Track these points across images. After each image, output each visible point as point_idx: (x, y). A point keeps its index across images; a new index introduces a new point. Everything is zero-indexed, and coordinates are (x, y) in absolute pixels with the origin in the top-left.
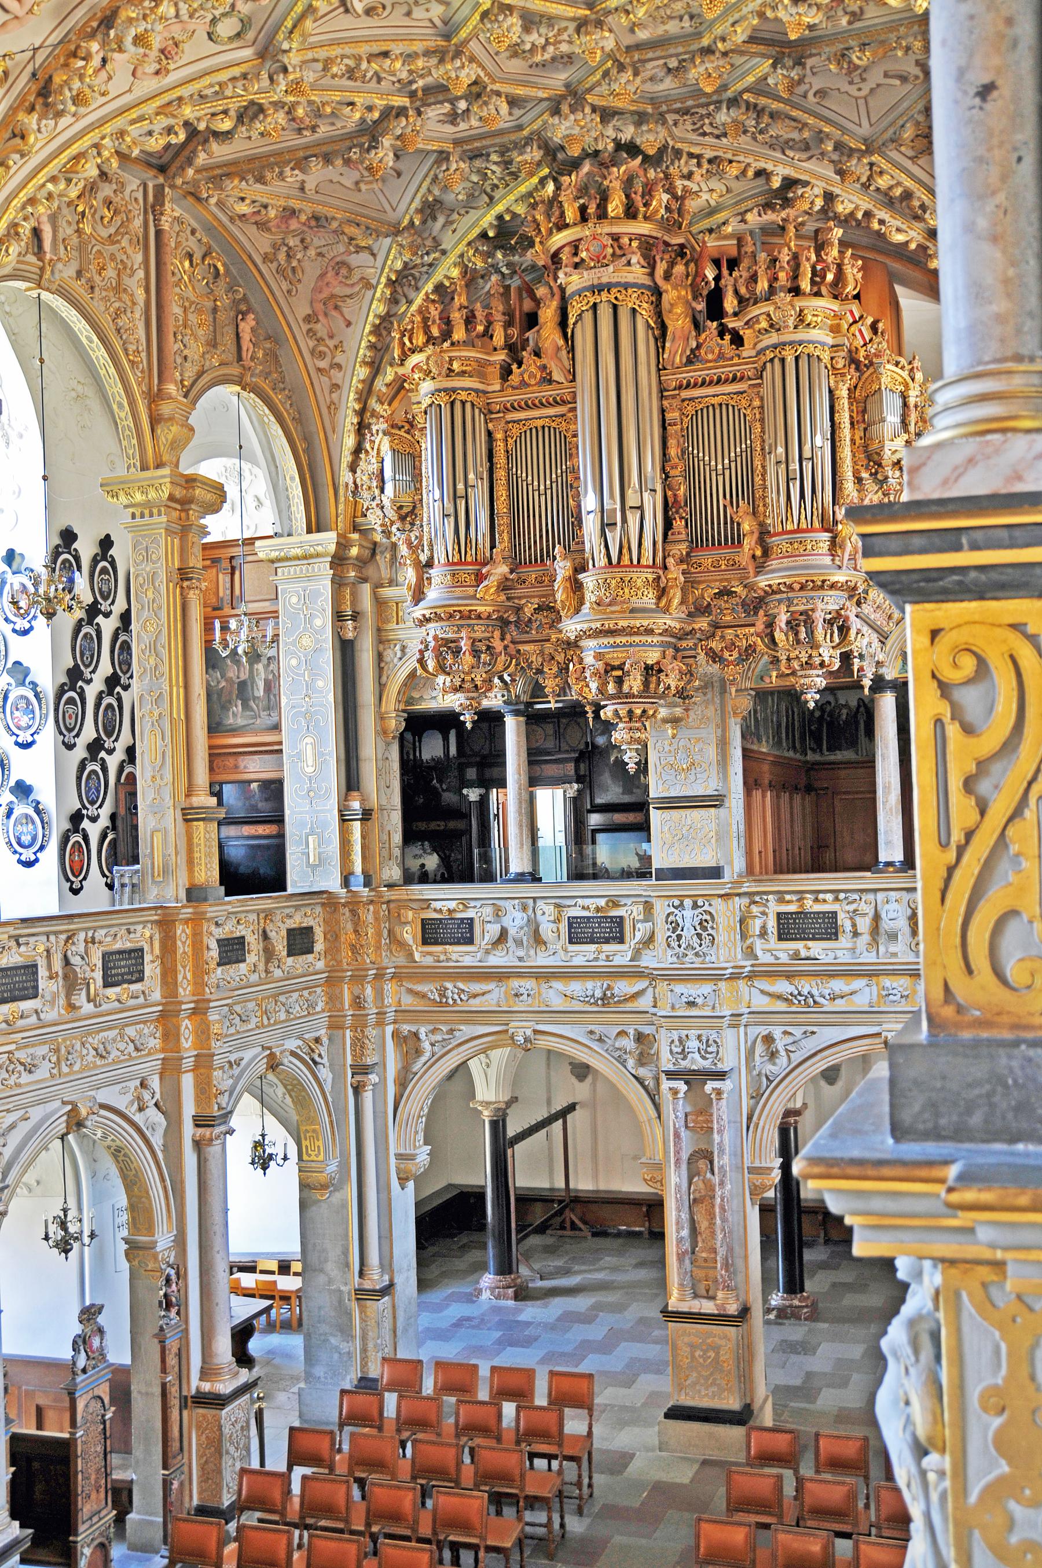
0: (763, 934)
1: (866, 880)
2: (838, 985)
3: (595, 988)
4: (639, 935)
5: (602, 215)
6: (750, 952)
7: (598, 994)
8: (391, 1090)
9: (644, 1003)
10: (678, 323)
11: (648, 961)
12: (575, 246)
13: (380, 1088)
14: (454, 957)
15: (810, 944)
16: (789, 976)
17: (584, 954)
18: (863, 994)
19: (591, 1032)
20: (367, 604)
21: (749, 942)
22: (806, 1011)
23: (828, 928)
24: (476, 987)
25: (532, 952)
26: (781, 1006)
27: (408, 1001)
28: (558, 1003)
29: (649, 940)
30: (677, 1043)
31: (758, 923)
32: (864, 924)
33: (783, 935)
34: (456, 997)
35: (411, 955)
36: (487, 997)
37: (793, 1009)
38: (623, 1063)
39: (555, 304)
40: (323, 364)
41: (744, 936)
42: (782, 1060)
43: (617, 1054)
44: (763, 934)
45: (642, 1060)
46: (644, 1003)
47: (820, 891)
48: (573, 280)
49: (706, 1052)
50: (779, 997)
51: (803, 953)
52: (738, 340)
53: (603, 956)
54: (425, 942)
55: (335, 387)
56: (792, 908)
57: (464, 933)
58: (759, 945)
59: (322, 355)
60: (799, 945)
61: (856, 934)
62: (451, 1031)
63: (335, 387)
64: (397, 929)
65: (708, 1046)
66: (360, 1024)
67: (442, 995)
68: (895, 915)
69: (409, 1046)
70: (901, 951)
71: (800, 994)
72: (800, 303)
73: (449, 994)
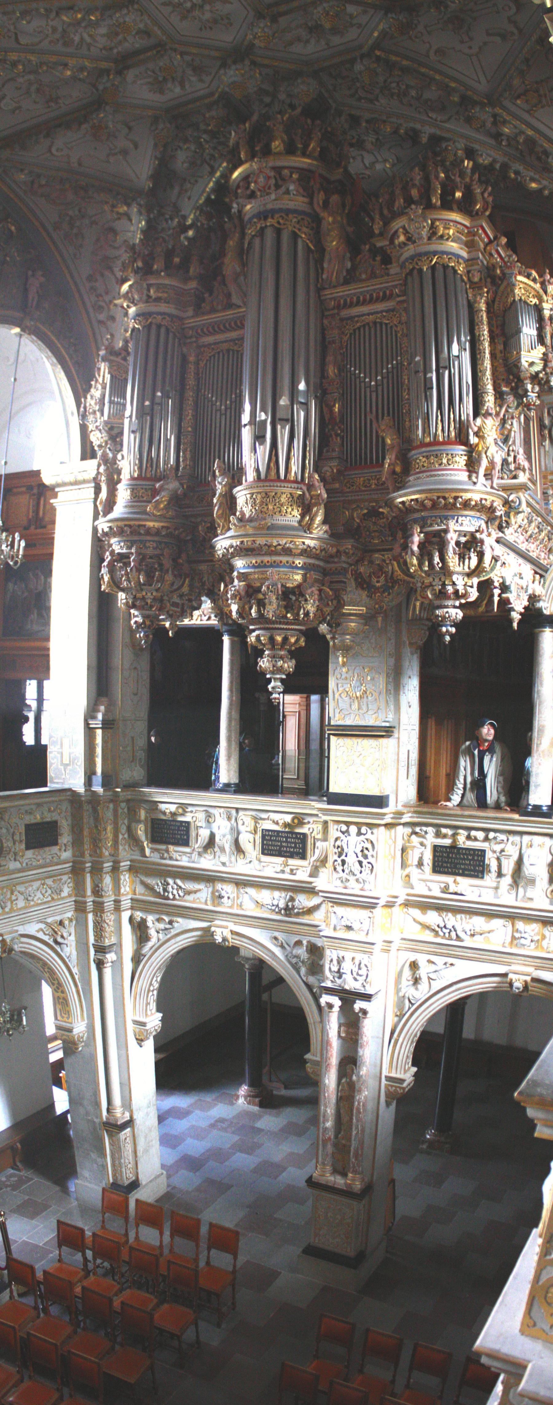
0: (420, 864)
3: (280, 898)
4: (317, 852)
7: (282, 905)
8: (128, 966)
13: (118, 965)
14: (175, 855)
15: (459, 879)
16: (440, 909)
17: (272, 867)
19: (276, 938)
21: (407, 871)
24: (190, 886)
25: (233, 858)
28: (250, 909)
30: (335, 962)
33: (438, 868)
34: (175, 892)
36: (198, 895)
37: (439, 940)
38: (298, 972)
41: (404, 865)
43: (294, 961)
44: (420, 864)
49: (358, 974)
50: (427, 927)
51: (452, 888)
53: (287, 869)
60: (449, 879)
64: (133, 824)
65: (360, 968)
66: (99, 908)
67: (165, 890)
71: (445, 927)
73: (170, 889)
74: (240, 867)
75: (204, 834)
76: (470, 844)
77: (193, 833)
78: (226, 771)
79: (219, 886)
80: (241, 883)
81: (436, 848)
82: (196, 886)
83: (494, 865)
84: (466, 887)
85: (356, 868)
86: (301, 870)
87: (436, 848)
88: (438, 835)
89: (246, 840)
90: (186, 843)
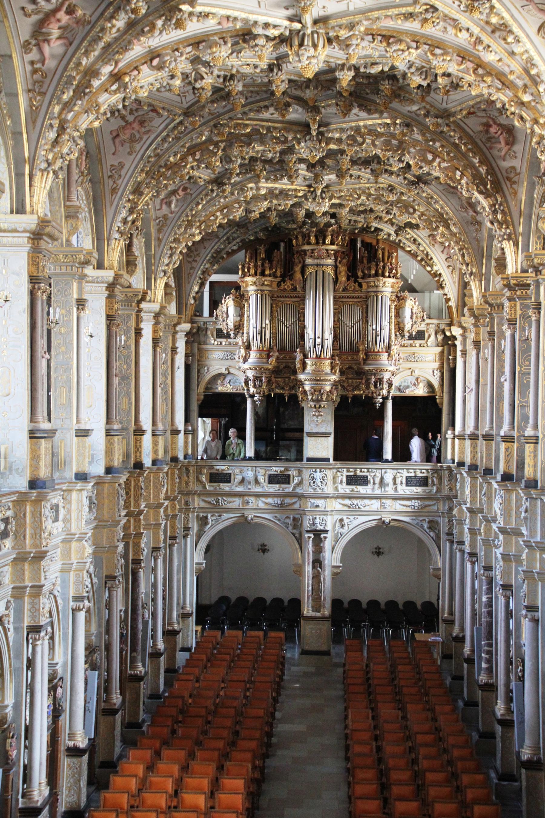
1: (380, 465)
2: (367, 502)
3: (278, 501)
5: (324, 243)
6: (336, 489)
9: (297, 506)
10: (343, 278)
11: (299, 490)
12: (313, 251)
16: (350, 498)
17: (274, 488)
18: (375, 505)
20: (196, 351)
22: (355, 511)
23: (364, 481)
24: (230, 499)
26: (346, 508)
27: (202, 504)
28: (261, 505)
29: (300, 483)
31: (340, 479)
32: (377, 480)
35: (205, 487)
39: (300, 266)
40: (190, 260)
42: (346, 528)
44: (341, 482)
45: (295, 527)
46: (297, 506)
47: (362, 468)
48: (309, 261)
52: (360, 285)
54: (211, 481)
55: (192, 268)
56: (352, 474)
57: (226, 478)
58: (340, 486)
59: (191, 257)
60: (354, 487)
61: (374, 484)
62: (220, 516)
63: (192, 268)
68: (389, 477)
69: (203, 521)
70: (390, 490)
72: (385, 280)
74: (258, 489)
75: (239, 478)
76: (361, 474)
77: (232, 477)
78: (250, 452)
79: (246, 498)
80: (258, 496)
81: (347, 476)
82: (234, 499)
83: (372, 481)
84: (362, 489)
85: (320, 484)
86: (289, 488)
87: (347, 476)
88: (348, 471)
89: (261, 479)
90: (229, 482)
